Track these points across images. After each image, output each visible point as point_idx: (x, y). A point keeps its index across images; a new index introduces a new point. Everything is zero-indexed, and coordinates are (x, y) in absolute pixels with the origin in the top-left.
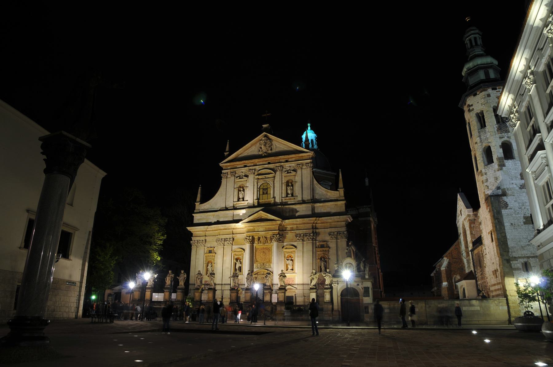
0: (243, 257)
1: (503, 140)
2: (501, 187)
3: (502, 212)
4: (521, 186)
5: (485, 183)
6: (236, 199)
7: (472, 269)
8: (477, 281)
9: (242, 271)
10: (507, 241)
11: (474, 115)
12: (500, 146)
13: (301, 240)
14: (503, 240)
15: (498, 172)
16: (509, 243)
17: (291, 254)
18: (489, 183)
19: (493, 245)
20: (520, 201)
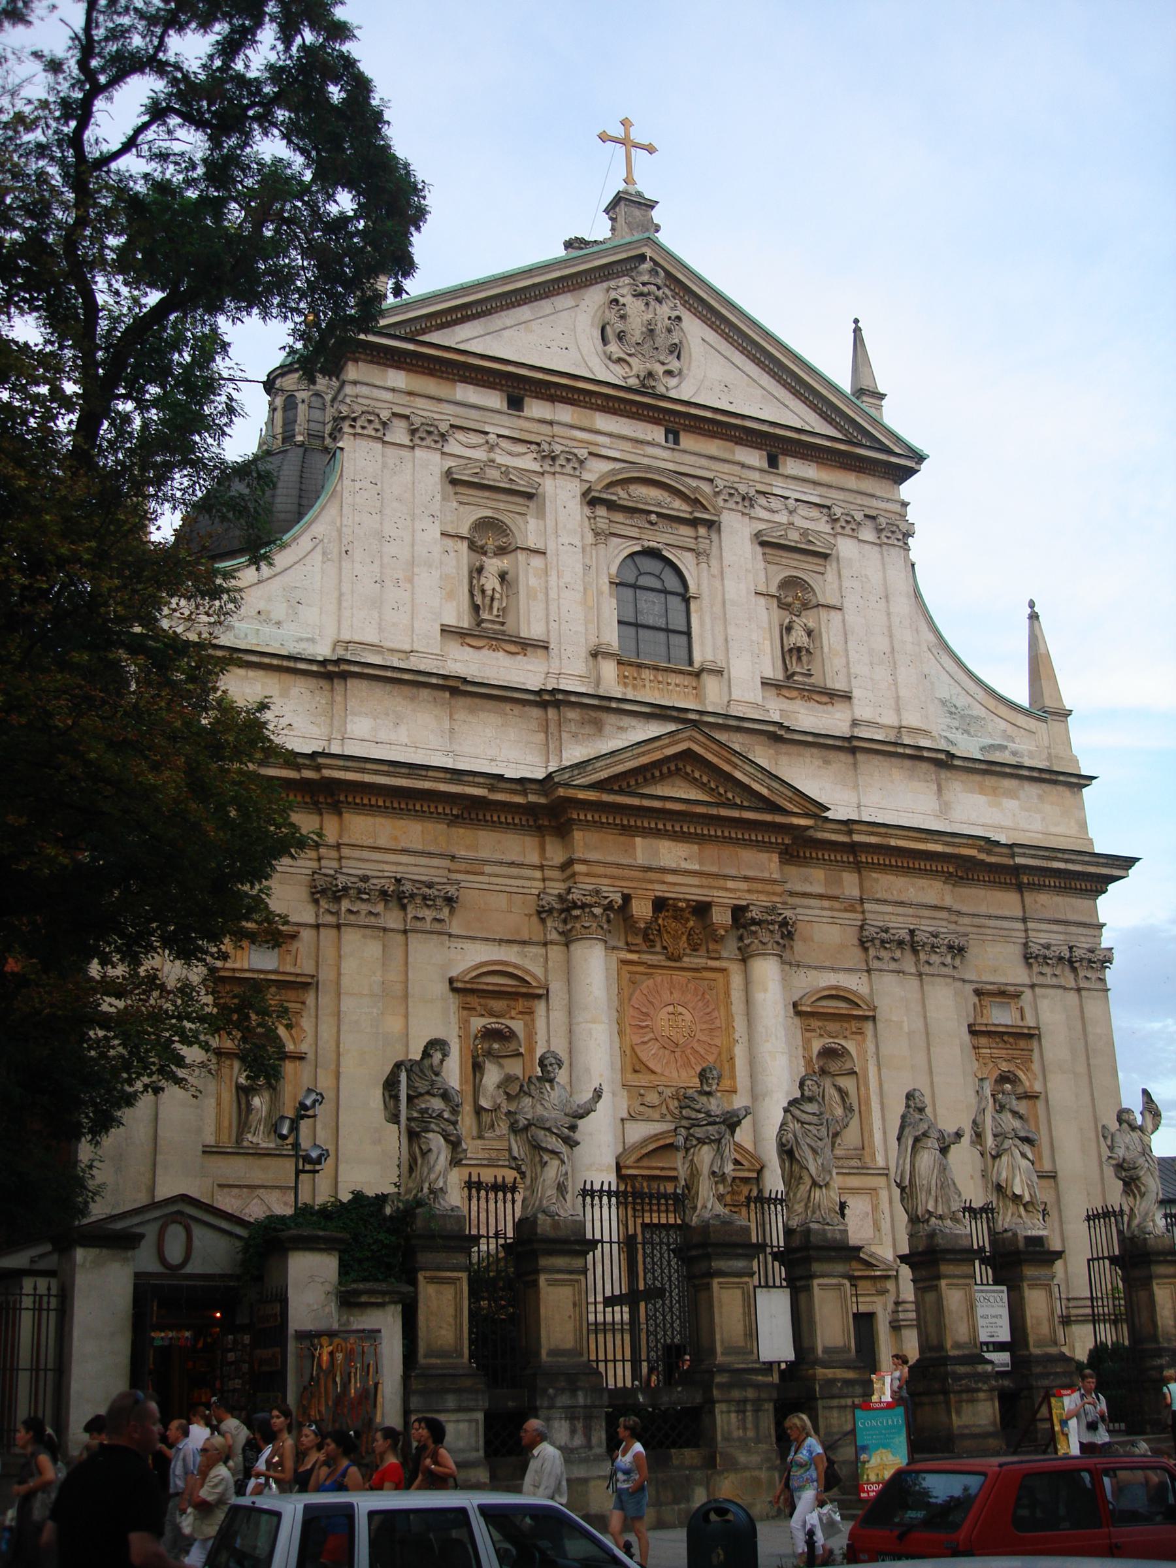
13: (893, 966)
17: (843, 1042)
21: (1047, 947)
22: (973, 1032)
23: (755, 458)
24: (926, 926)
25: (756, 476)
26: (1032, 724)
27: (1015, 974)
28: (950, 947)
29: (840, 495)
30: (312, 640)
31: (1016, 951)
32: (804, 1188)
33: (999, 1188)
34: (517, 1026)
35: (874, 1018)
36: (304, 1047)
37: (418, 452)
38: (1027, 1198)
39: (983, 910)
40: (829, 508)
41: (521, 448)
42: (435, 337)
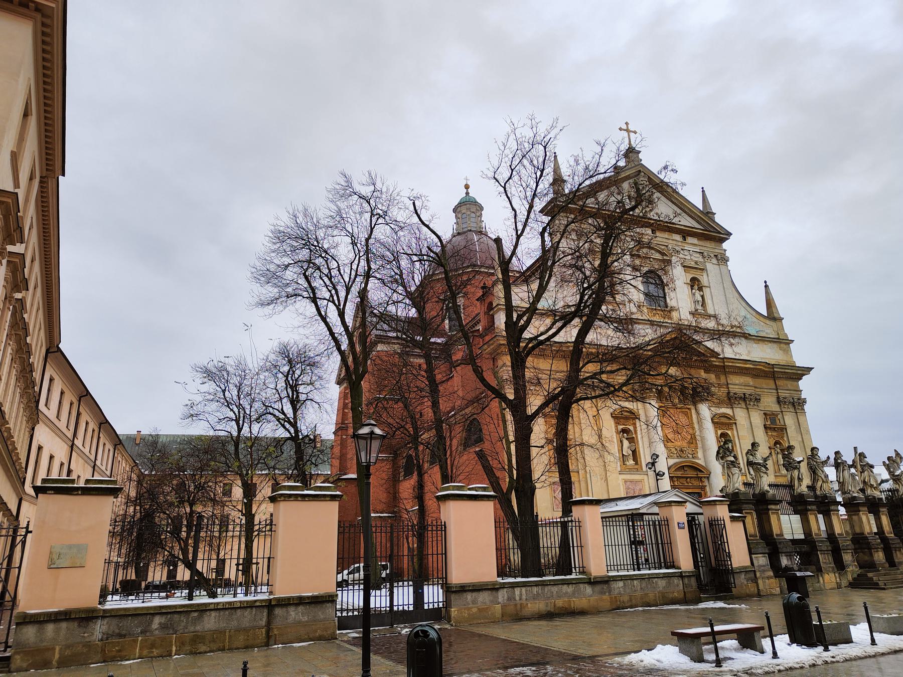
9: (639, 463)
17: (727, 431)
21: (785, 398)
22: (765, 427)
23: (678, 237)
24: (748, 391)
25: (680, 244)
27: (775, 408)
28: (756, 399)
29: (705, 249)
31: (774, 399)
32: (820, 483)
33: (864, 482)
34: (631, 428)
35: (736, 423)
38: (875, 486)
40: (702, 253)
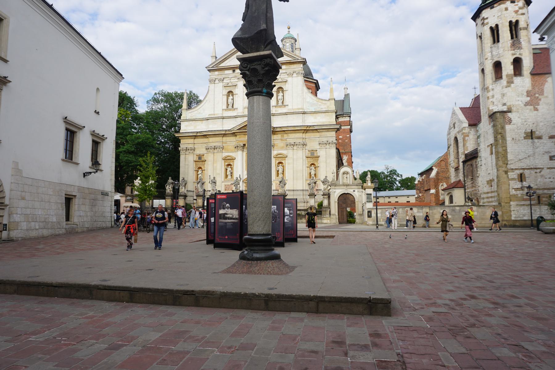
0: (233, 163)
1: (515, 56)
2: (506, 104)
3: (506, 128)
4: (526, 103)
5: (491, 99)
6: (225, 107)
7: (461, 178)
8: (465, 190)
10: (507, 154)
11: (489, 27)
12: (511, 62)
13: (292, 148)
14: (503, 154)
15: (506, 89)
16: (509, 156)
18: (495, 99)
19: (492, 157)
20: (523, 117)
21: (323, 142)
24: (297, 141)
26: (326, 102)
27: (317, 147)
30: (206, 115)
34: (231, 163)
36: (205, 169)
37: (219, 84)
39: (312, 137)
41: (235, 78)
42: (222, 65)
